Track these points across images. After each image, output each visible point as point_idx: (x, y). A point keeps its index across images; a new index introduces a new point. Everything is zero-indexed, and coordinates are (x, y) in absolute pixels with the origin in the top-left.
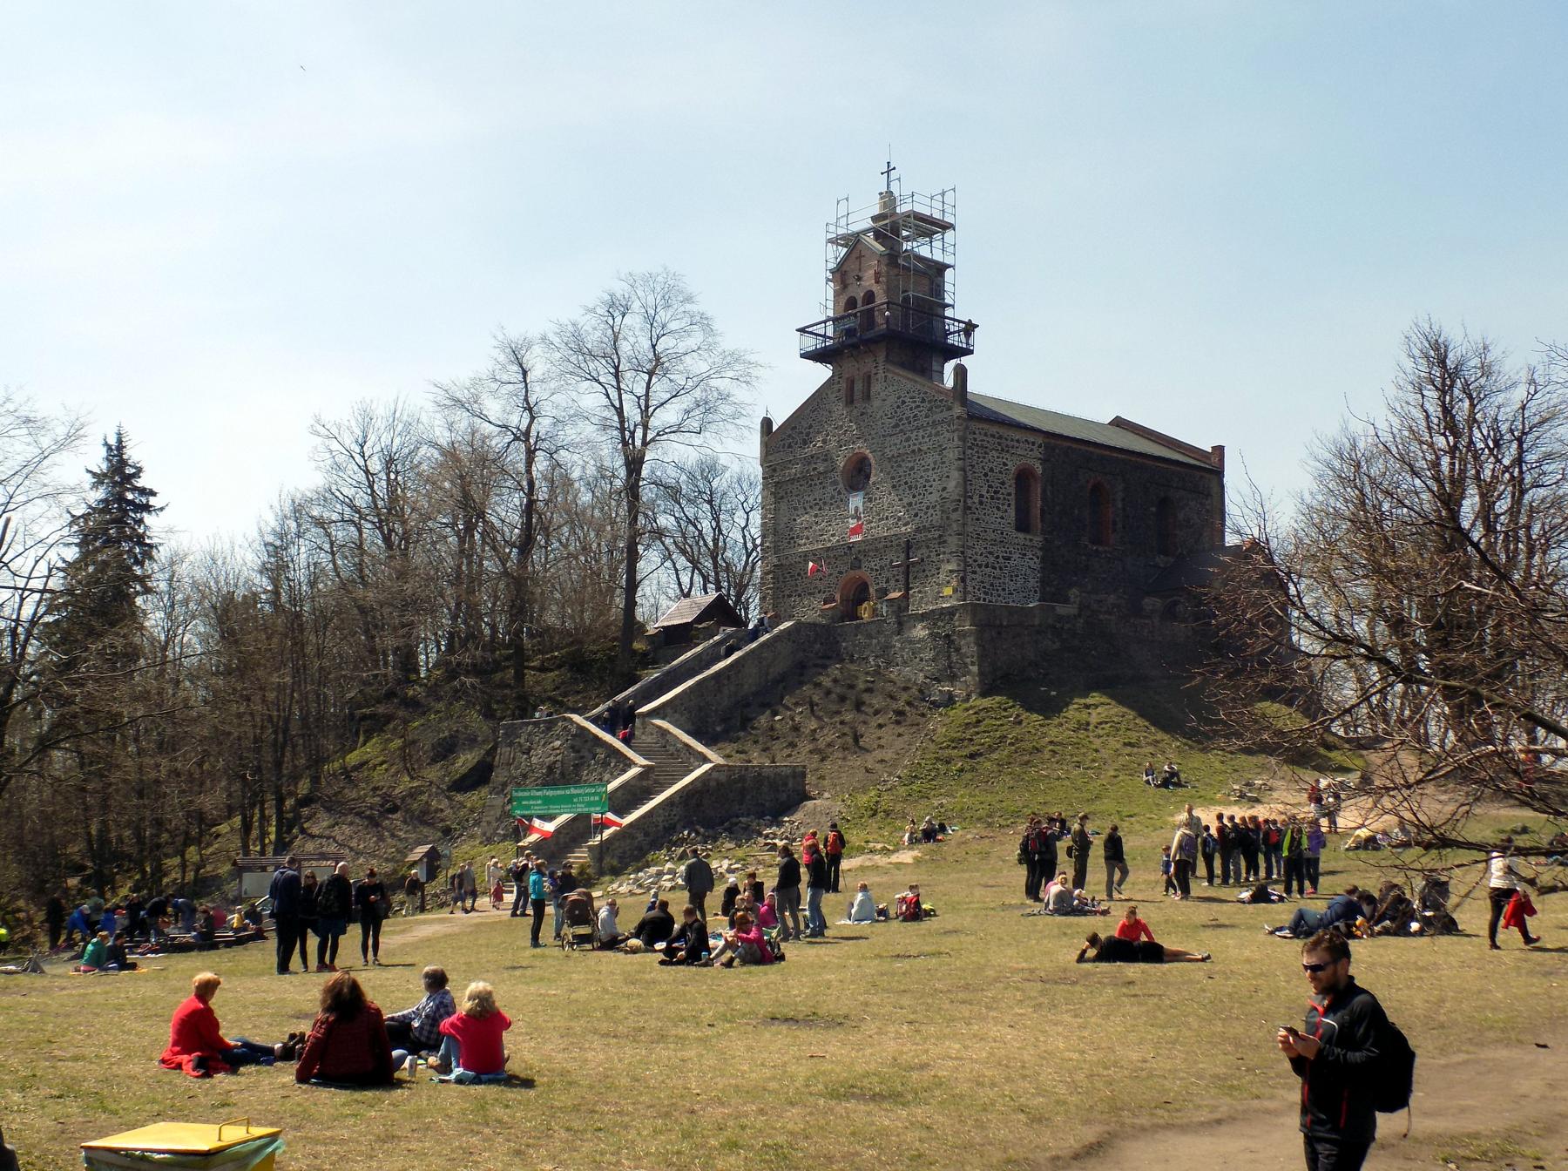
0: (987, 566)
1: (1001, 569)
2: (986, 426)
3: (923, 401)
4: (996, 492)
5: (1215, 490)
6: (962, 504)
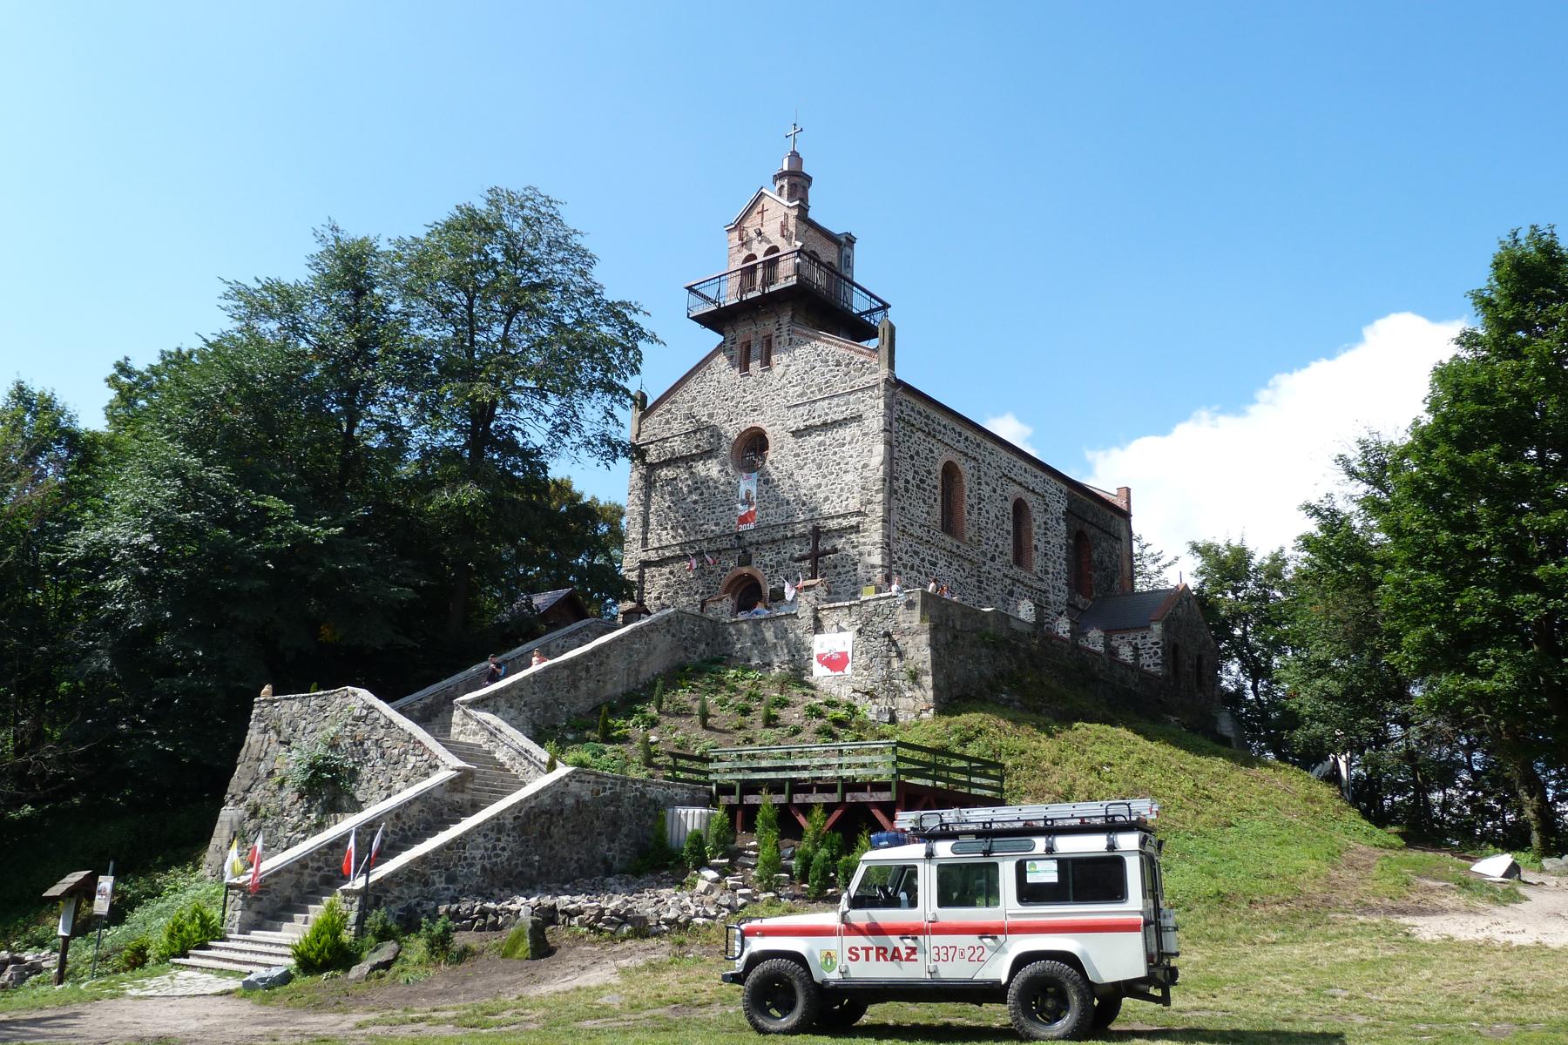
0: (912, 568)
1: (927, 575)
2: (913, 401)
3: (838, 364)
4: (922, 481)
5: (1124, 534)
6: (887, 484)
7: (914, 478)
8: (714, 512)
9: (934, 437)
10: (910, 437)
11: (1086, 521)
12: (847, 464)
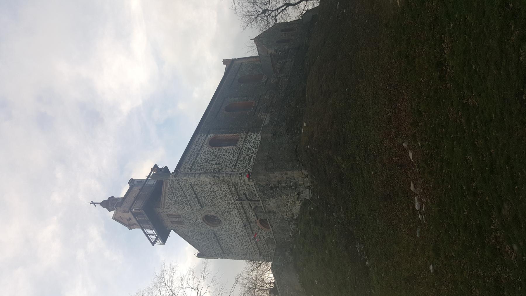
0: (250, 160)
1: (253, 153)
5: (240, 61)
6: (216, 175)
7: (215, 161)
8: (238, 232)
9: (199, 151)
10: (199, 163)
12: (211, 189)
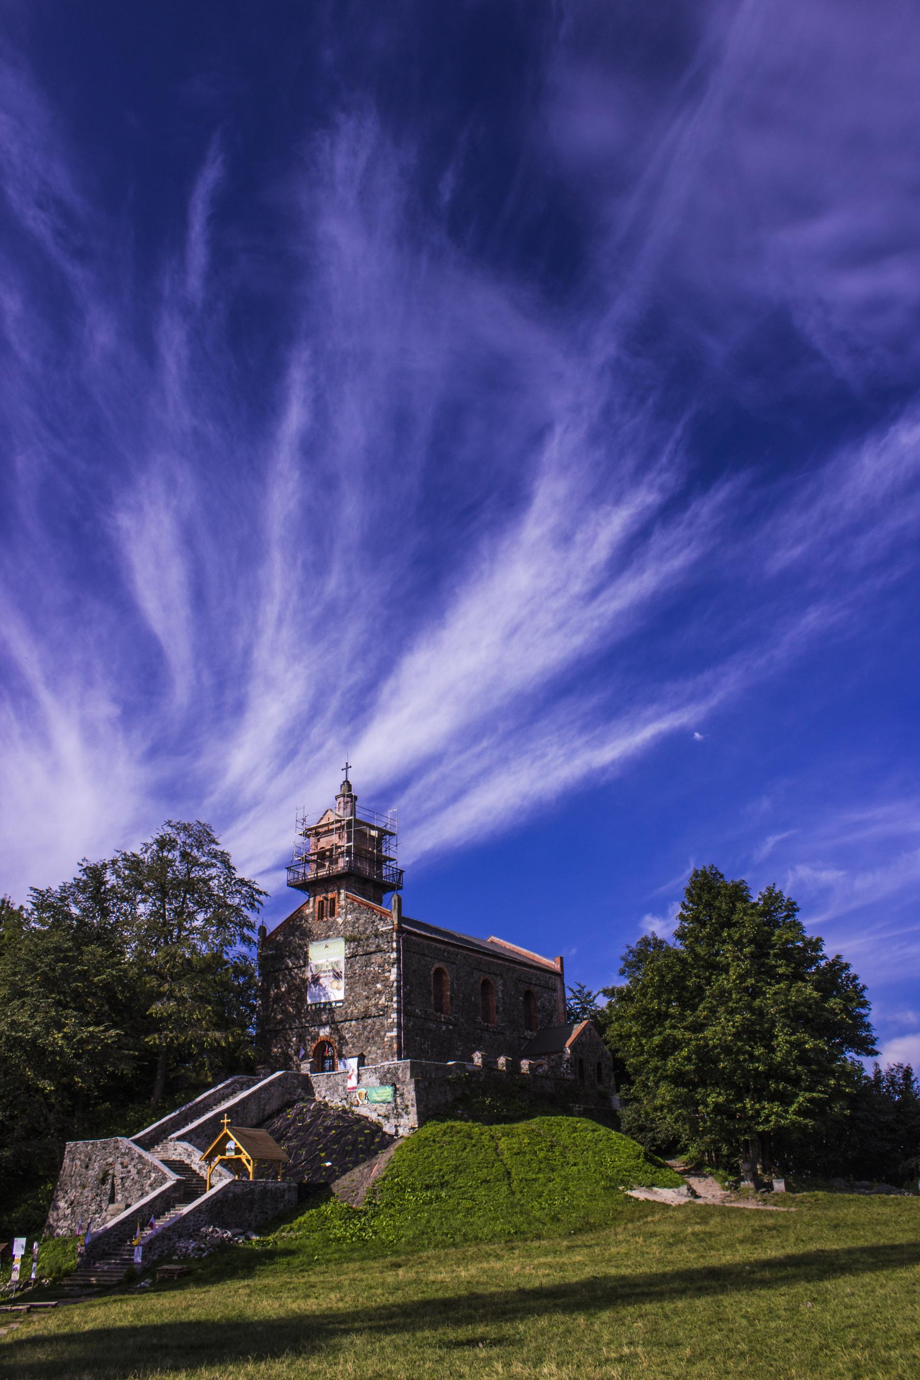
5: (559, 986)
11: (531, 984)
